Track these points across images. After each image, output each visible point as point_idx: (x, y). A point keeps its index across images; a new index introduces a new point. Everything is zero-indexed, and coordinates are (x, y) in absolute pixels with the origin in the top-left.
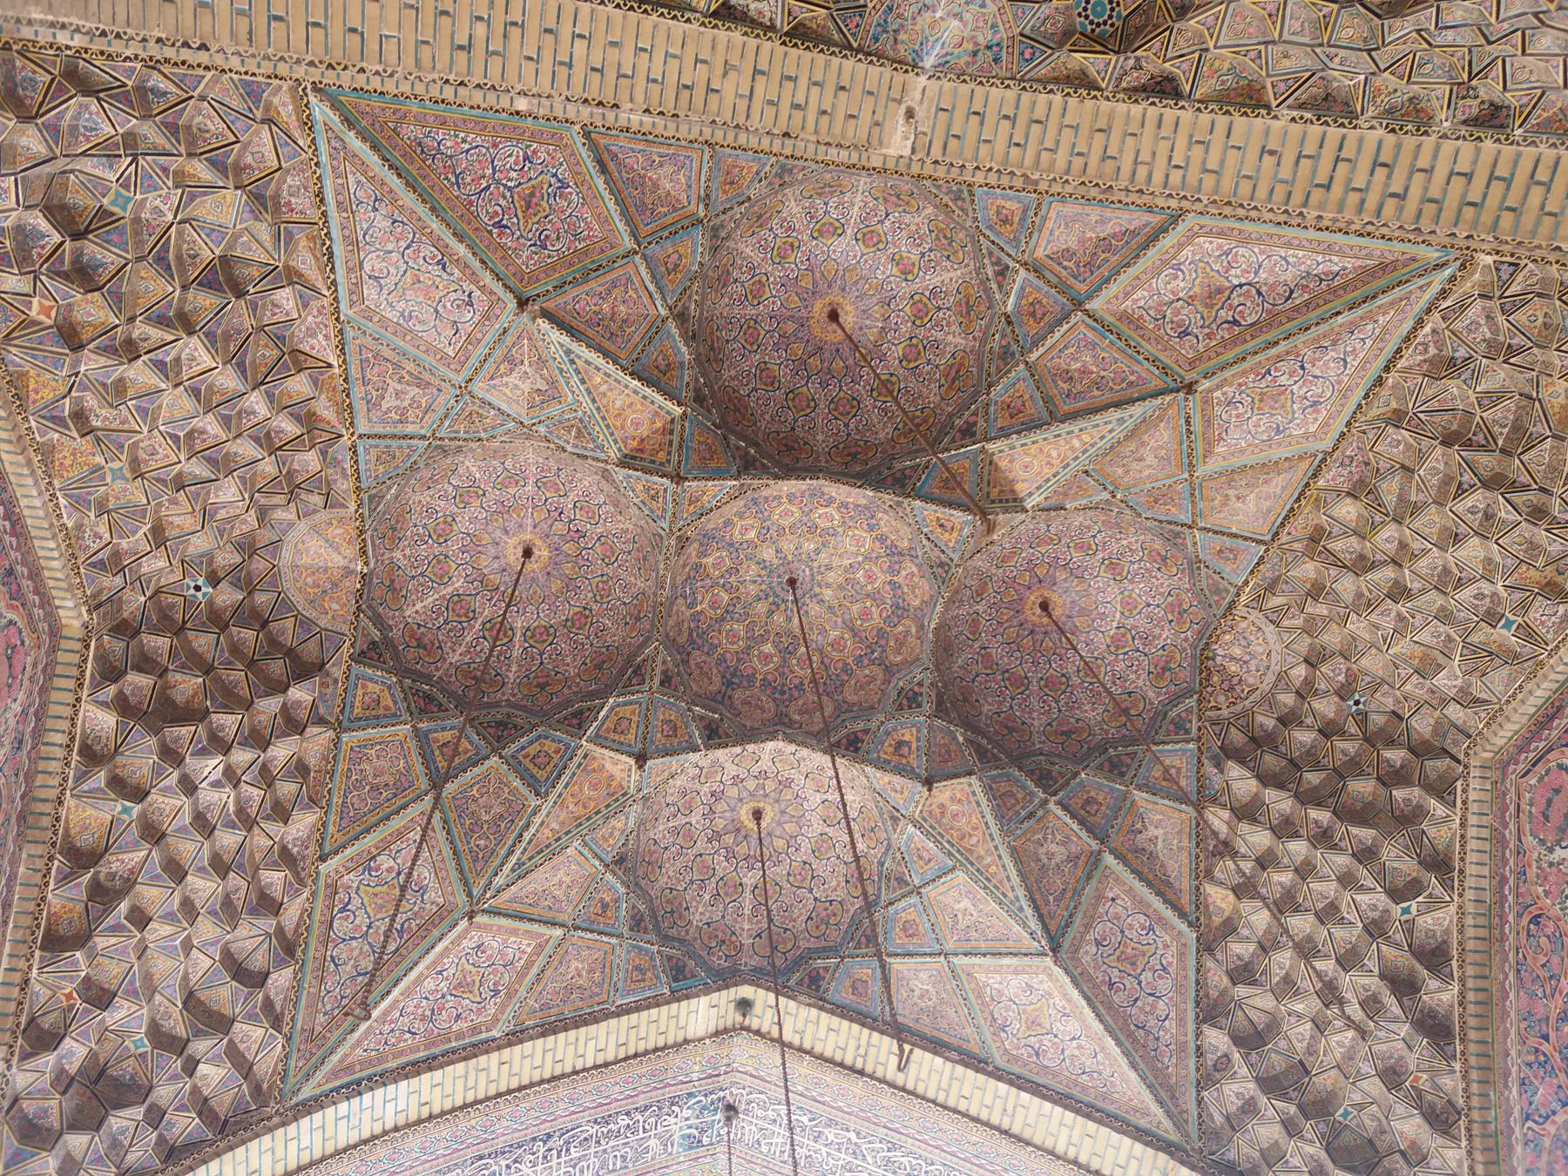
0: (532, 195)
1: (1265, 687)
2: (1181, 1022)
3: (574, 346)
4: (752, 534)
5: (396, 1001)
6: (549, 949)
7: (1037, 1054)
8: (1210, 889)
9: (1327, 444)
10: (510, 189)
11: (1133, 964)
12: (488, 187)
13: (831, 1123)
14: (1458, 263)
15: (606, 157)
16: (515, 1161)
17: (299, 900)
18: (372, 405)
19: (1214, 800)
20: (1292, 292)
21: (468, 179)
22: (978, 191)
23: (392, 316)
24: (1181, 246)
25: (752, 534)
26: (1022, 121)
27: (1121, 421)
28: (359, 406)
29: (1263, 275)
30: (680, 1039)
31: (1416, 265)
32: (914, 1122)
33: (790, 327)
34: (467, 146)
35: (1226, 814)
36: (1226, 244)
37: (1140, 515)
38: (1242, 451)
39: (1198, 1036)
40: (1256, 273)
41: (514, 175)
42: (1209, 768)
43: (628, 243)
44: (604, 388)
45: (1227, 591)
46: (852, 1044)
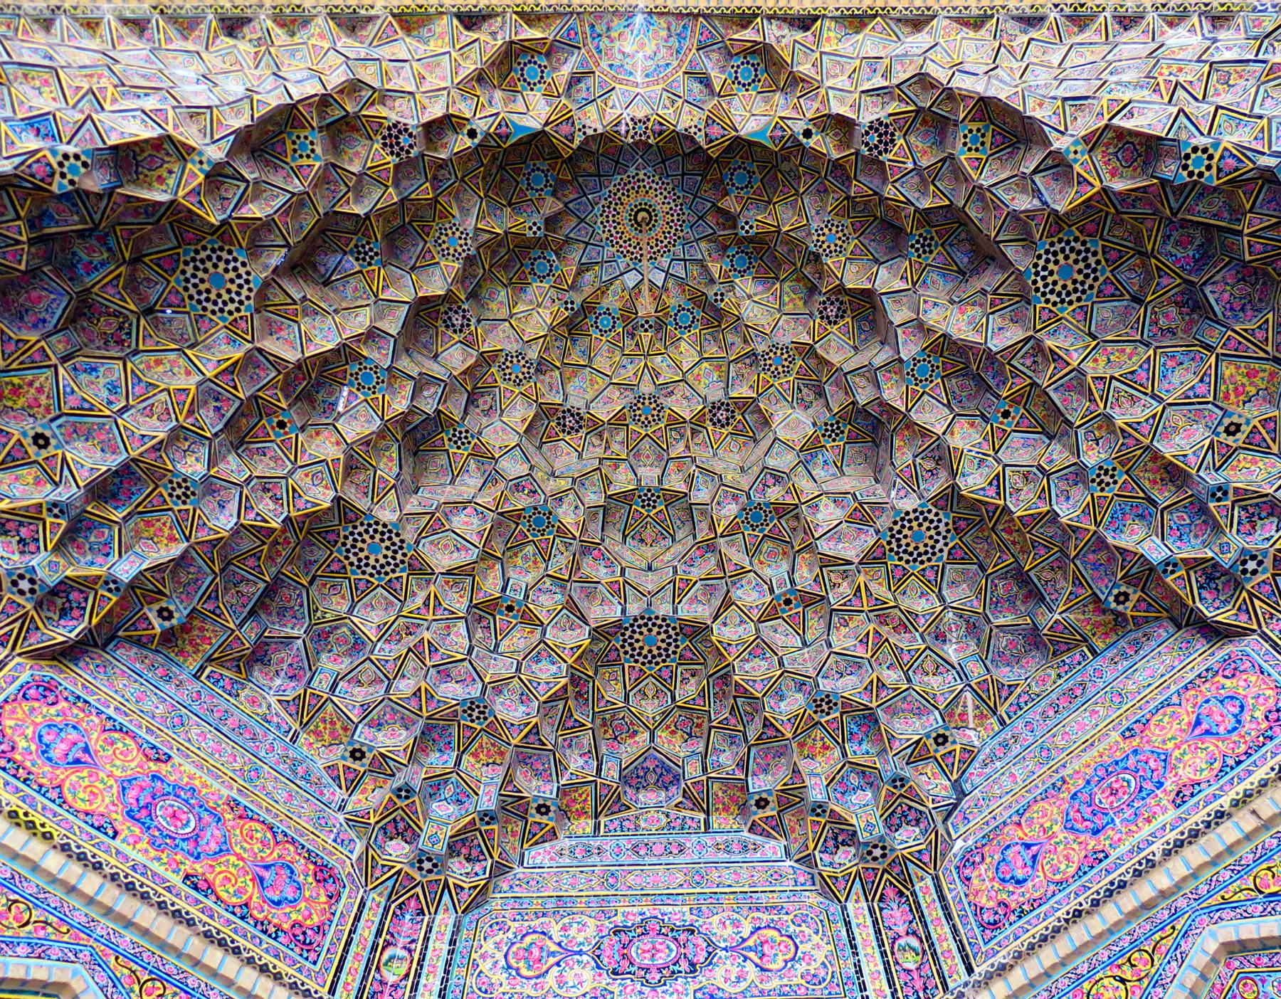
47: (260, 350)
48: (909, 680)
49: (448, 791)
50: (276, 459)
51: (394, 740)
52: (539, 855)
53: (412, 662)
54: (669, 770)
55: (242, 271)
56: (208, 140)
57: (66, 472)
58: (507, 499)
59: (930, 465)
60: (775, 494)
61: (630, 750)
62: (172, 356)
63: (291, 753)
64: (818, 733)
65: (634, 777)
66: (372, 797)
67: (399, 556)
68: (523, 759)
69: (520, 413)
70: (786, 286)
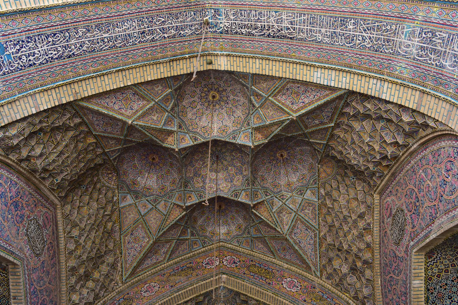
1: (100, 172)
2: (88, 119)
3: (275, 227)
4: (230, 168)
5: (316, 102)
6: (273, 95)
7: (122, 93)
8: (95, 141)
9: (122, 236)
11: (106, 124)
13: (174, 36)
16: (279, 30)
17: (340, 120)
18: (314, 208)
19: (101, 154)
22: (202, 247)
23: (309, 230)
24: (165, 257)
25: (230, 168)
27: (163, 229)
28: (317, 209)
30: (229, 57)
32: (149, 53)
33: (229, 204)
35: (98, 153)
36: (158, 261)
37: (147, 200)
38: (136, 227)
39: (83, 120)
42: (106, 158)
43: (266, 238)
44: (269, 217)
45: (120, 190)
46: (175, 68)
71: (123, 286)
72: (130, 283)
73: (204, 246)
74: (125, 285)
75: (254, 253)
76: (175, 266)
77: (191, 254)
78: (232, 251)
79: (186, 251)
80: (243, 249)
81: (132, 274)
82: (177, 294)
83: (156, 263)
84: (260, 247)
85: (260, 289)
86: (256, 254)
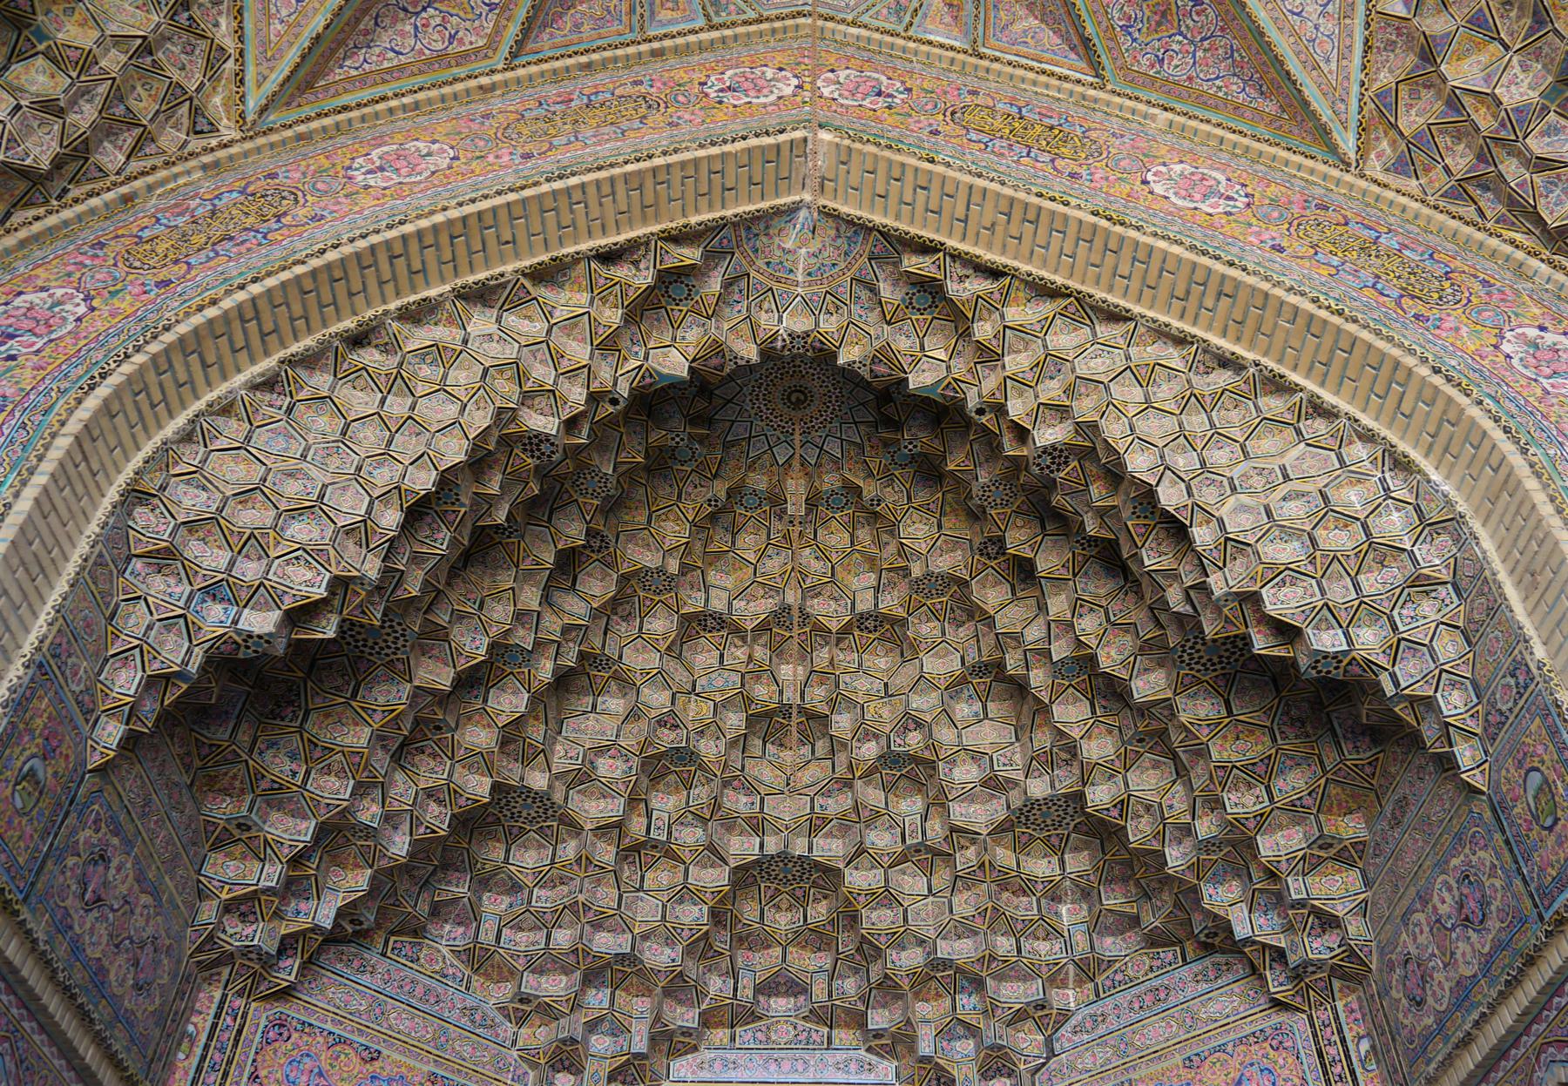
0: (1159, 24)
10: (1181, 34)
12: (1203, 40)
14: (249, 119)
15: (1080, 49)
20: (376, 24)
21: (1221, 51)
22: (701, 22)
26: (717, 190)
29: (409, 28)
31: (283, 100)
34: (1218, 82)
36: (455, 48)
40: (416, 27)
41: (1175, 47)
47: (418, 687)
48: (1019, 951)
49: (606, 1026)
50: (434, 756)
51: (554, 986)
52: (682, 1067)
53: (568, 916)
54: (798, 985)
55: (398, 628)
56: (364, 551)
57: (269, 851)
58: (650, 744)
59: (1064, 756)
60: (914, 740)
61: (764, 962)
62: (339, 709)
63: (470, 1003)
64: (933, 984)
65: (770, 987)
66: (538, 1035)
67: (550, 812)
68: (667, 992)
69: (661, 624)
70: (949, 496)
71: (248, 145)
72: (289, 133)
73: (716, 20)
74: (261, 141)
75: (985, 63)
76: (552, 91)
77: (644, 47)
78: (865, 54)
79: (616, 27)
80: (925, 48)
81: (305, 79)
82: (558, 185)
83: (441, 58)
84: (1018, 27)
85: (1021, 195)
86: (996, 66)
